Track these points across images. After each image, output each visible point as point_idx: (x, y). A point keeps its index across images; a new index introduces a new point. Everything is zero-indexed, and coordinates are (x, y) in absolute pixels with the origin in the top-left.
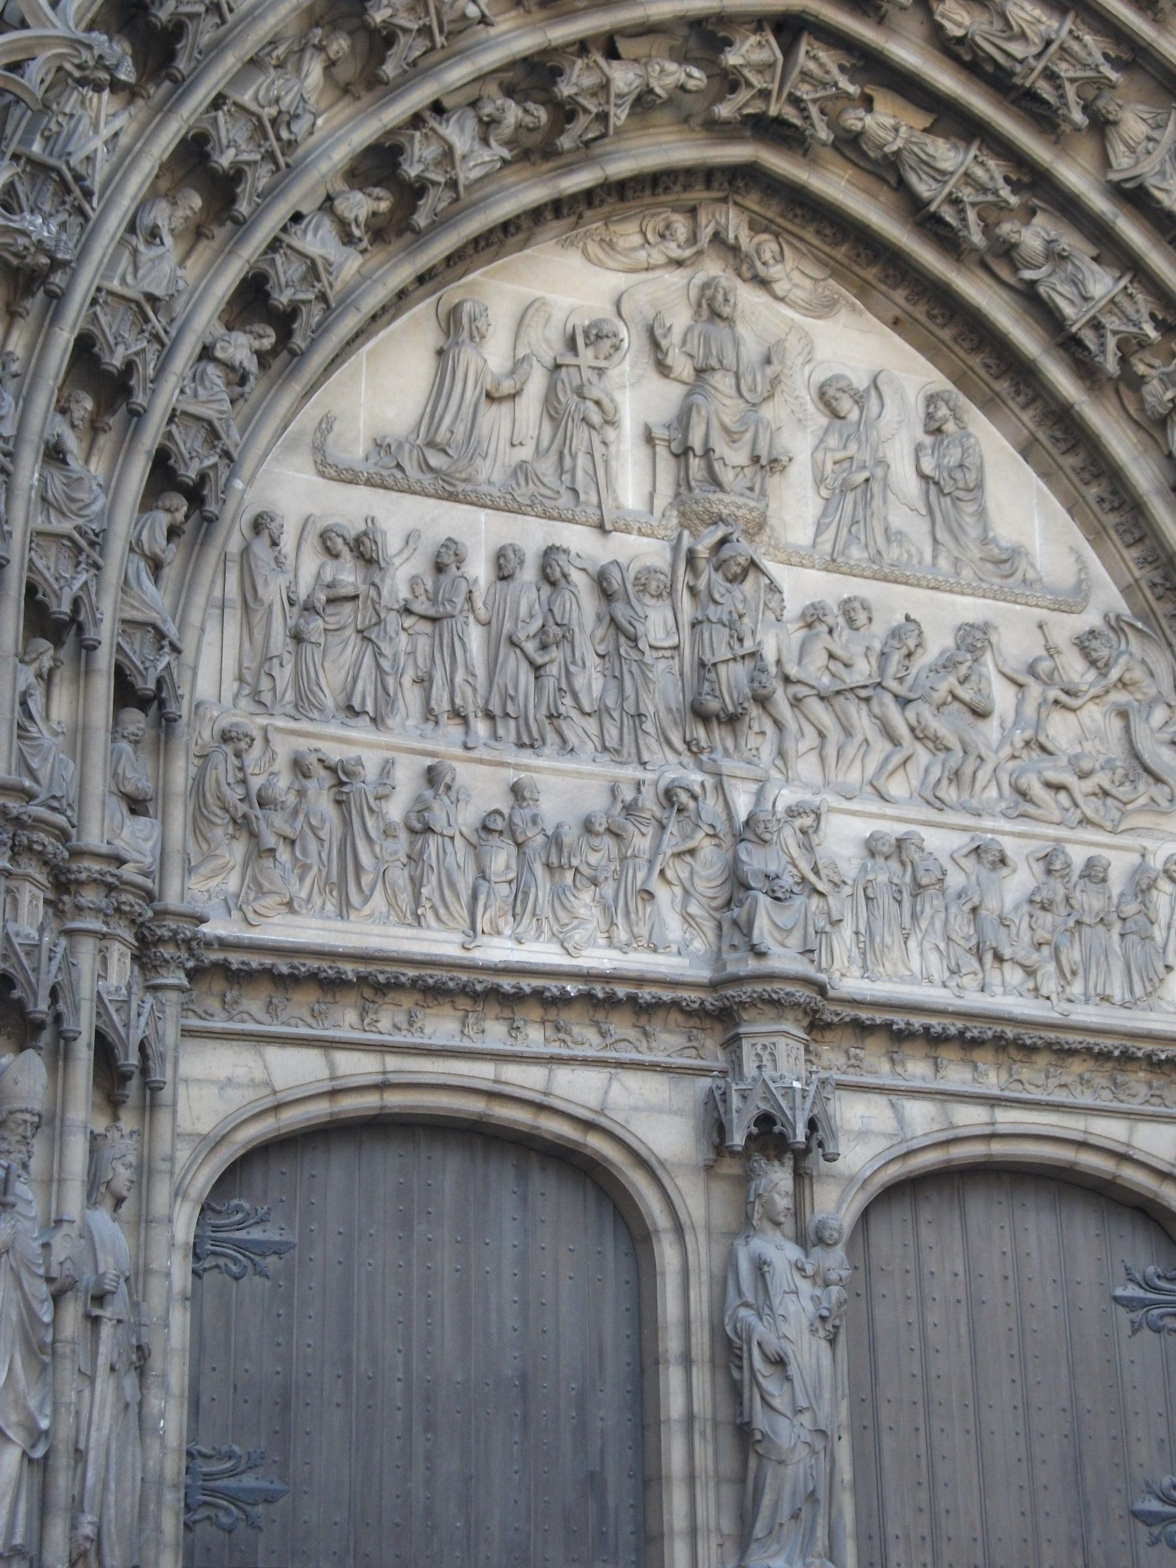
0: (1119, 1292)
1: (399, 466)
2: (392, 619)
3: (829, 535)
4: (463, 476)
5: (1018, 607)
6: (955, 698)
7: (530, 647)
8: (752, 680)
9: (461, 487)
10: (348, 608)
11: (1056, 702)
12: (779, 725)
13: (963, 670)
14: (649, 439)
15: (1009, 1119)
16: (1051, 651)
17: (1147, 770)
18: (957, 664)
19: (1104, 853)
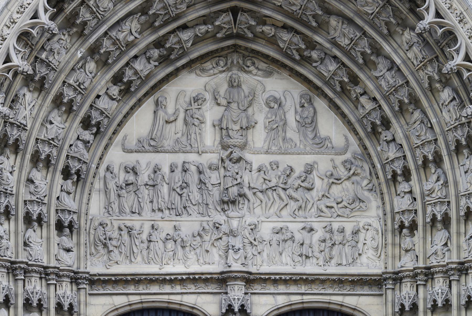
1: (143, 146)
2: (142, 188)
3: (267, 143)
4: (160, 146)
5: (325, 156)
6: (301, 186)
7: (178, 190)
8: (238, 191)
9: (159, 149)
10: (131, 186)
11: (333, 183)
12: (249, 200)
13: (303, 178)
14: (214, 126)
16: (335, 167)
17: (360, 199)
18: (300, 177)
19: (344, 224)
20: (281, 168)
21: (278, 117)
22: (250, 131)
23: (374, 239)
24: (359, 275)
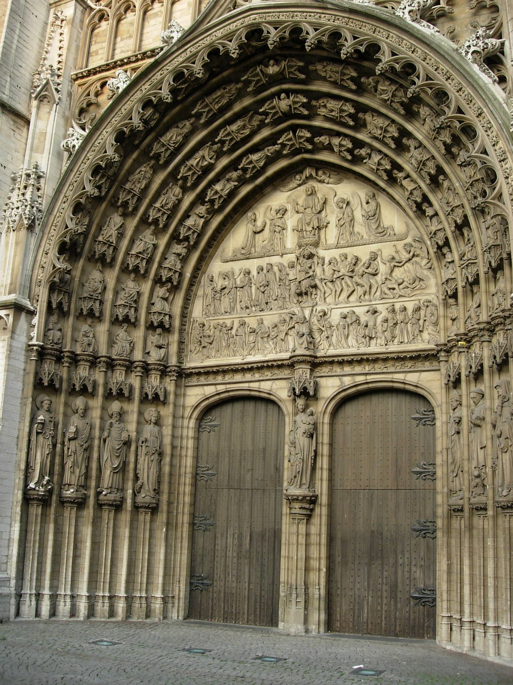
0: (413, 416)
11: (395, 266)
15: (370, 378)
16: (397, 252)
20: (349, 259)
21: (345, 214)
22: (322, 232)
23: (433, 315)
24: (417, 351)
